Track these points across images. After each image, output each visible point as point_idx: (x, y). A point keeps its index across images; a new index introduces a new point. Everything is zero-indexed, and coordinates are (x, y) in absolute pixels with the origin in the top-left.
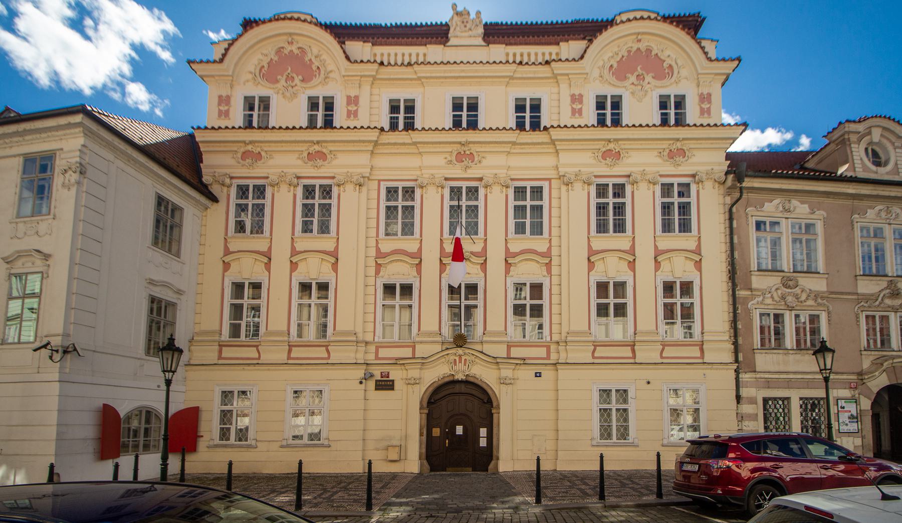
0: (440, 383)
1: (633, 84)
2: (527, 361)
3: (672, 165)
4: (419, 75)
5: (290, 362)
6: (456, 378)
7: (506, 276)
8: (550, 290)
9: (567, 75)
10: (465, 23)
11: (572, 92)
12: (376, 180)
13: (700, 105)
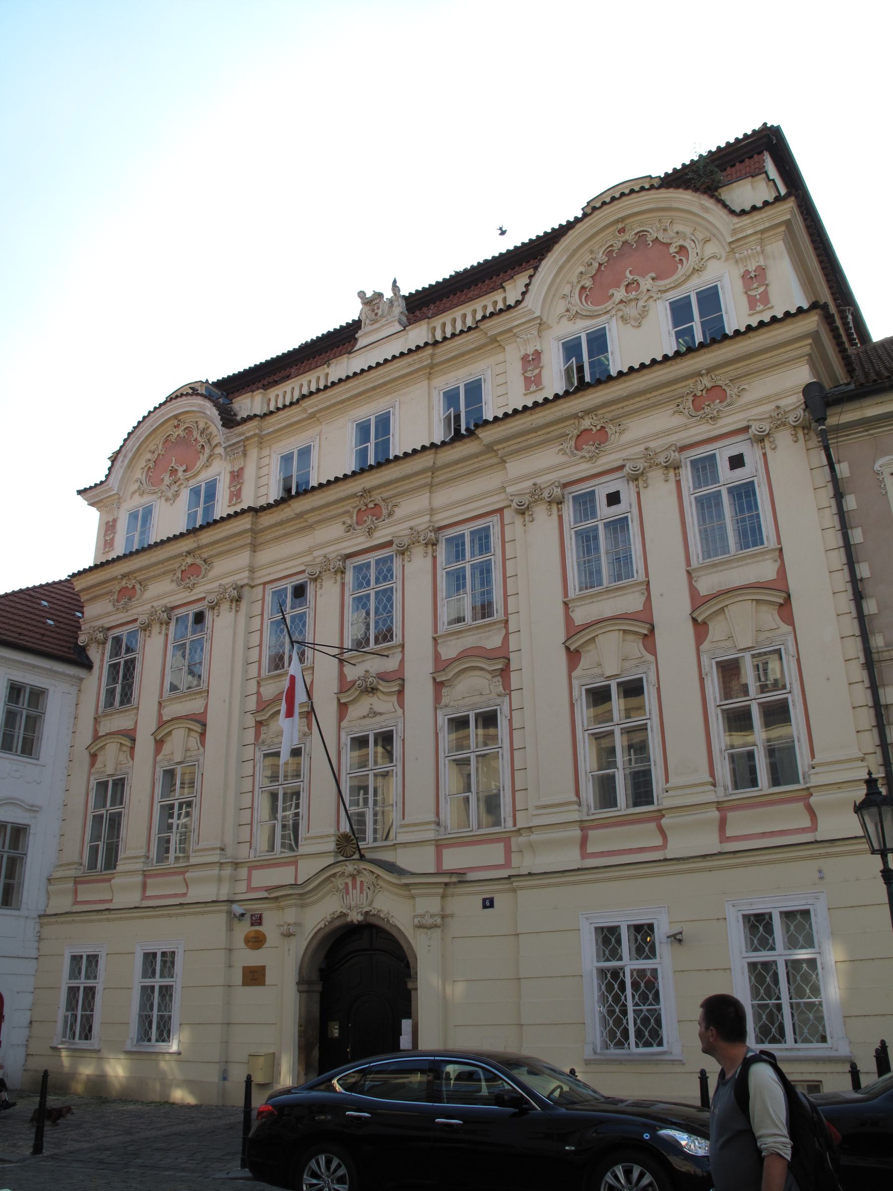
0: (327, 930)
1: (621, 301)
2: (471, 876)
3: (704, 421)
4: (310, 411)
5: (146, 903)
6: (349, 919)
7: (436, 709)
8: (510, 721)
9: (510, 330)
10: (376, 311)
11: (523, 353)
12: (260, 584)
13: (746, 293)
